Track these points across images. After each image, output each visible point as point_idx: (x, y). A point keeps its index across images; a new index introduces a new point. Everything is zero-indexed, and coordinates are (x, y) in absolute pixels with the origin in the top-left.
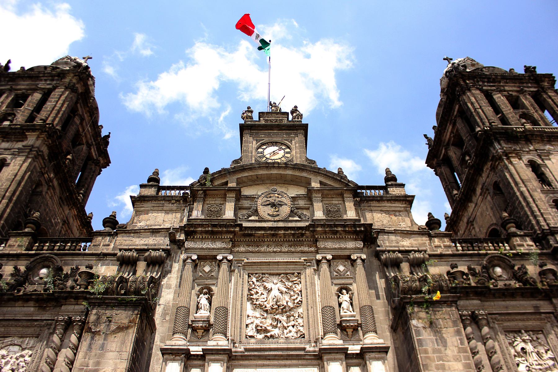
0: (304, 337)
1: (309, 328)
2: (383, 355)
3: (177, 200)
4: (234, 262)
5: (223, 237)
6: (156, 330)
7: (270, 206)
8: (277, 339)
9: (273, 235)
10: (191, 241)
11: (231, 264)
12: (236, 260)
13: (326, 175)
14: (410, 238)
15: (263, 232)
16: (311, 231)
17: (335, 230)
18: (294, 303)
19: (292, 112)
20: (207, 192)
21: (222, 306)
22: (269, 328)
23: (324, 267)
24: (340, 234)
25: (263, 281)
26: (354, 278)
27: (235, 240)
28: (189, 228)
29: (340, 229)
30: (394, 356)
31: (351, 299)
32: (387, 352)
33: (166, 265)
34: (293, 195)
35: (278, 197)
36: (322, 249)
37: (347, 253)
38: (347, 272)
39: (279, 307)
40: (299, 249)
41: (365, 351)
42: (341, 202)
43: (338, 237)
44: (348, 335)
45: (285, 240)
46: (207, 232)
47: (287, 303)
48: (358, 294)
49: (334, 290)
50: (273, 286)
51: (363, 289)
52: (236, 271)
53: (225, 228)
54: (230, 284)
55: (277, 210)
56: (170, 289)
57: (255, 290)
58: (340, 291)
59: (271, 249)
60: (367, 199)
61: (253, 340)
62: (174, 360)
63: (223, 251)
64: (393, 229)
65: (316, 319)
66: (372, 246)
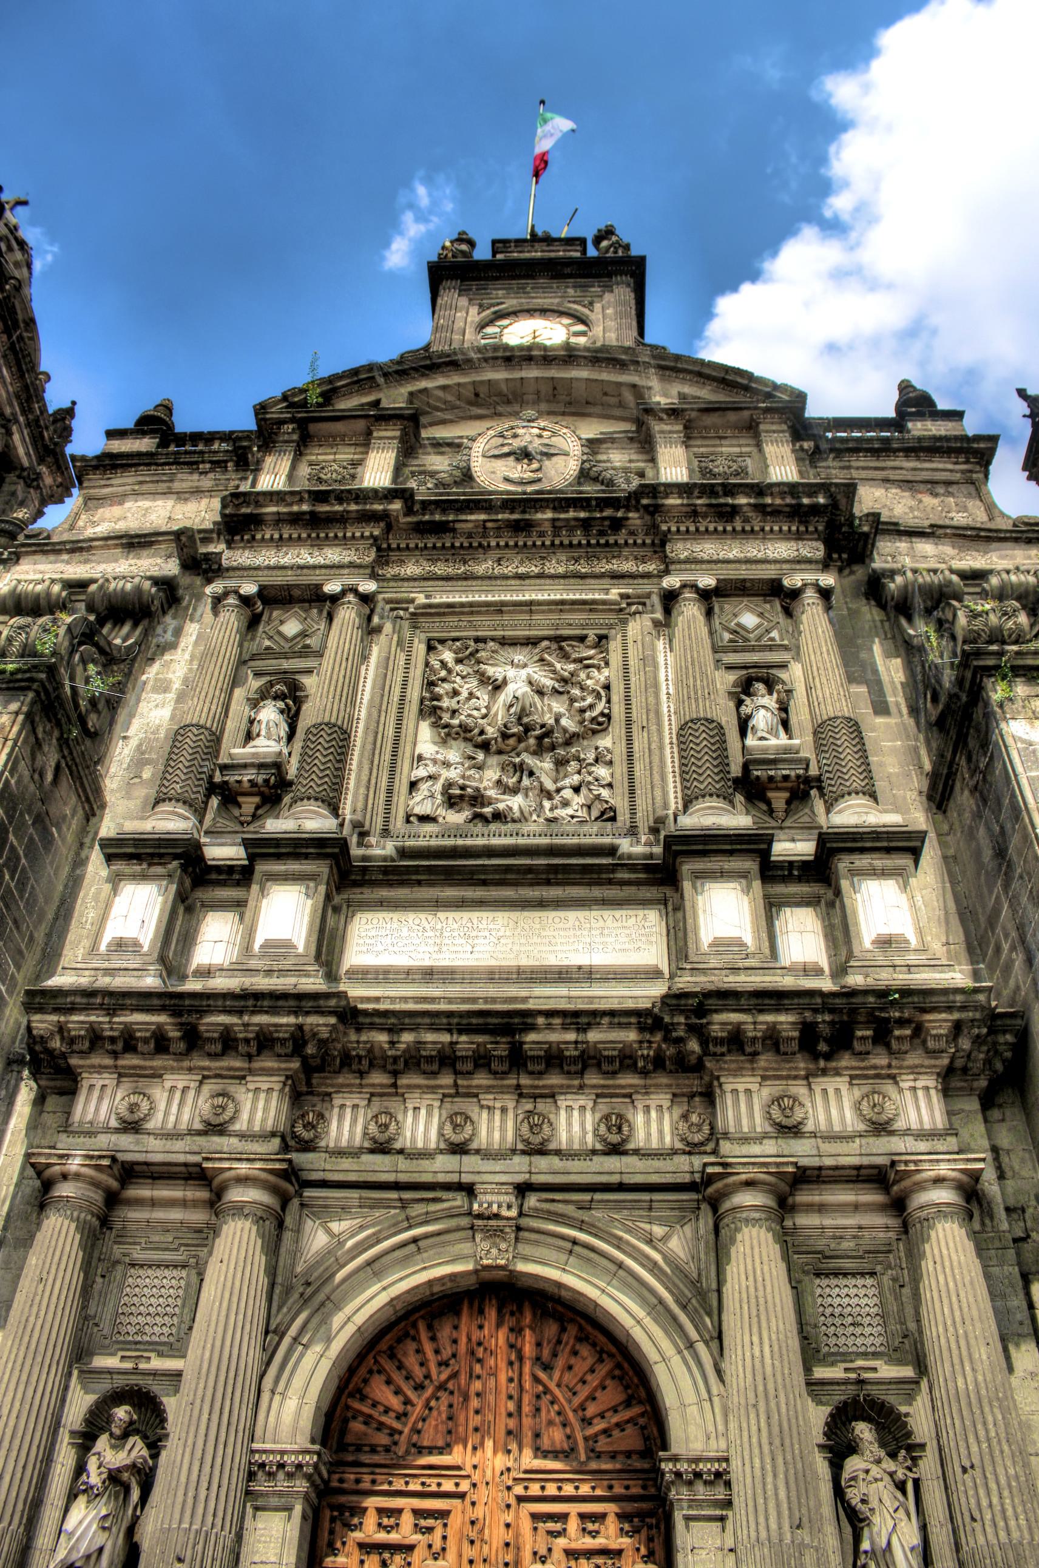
0: (613, 819)
1: (632, 792)
2: (906, 861)
3: (218, 462)
4: (380, 605)
5: (349, 534)
6: (103, 806)
7: (512, 458)
8: (518, 826)
9: (520, 527)
10: (244, 548)
11: (372, 611)
12: (388, 601)
13: (700, 374)
14: (986, 553)
15: (483, 517)
16: (646, 507)
17: (727, 505)
18: (581, 722)
19: (598, 240)
20: (313, 428)
21: (326, 720)
22: (492, 793)
23: (690, 611)
24: (746, 520)
25: (479, 662)
26: (796, 651)
27: (389, 545)
28: (237, 506)
29: (742, 500)
30: (943, 882)
31: (784, 708)
32: (915, 853)
33: (159, 630)
34: (591, 436)
35: (540, 436)
36: (680, 562)
37: (768, 572)
38: (768, 631)
39: (528, 729)
40: (604, 567)
41: (835, 845)
42: (748, 449)
43: (739, 528)
44: (771, 812)
45: (557, 542)
46: (295, 519)
47: (557, 721)
48: (809, 689)
49: (722, 683)
50: (511, 673)
51: (826, 669)
52: (388, 627)
53: (357, 503)
54: (364, 667)
55: (535, 466)
56: (165, 691)
57: (447, 686)
58: (745, 688)
59: (509, 569)
60: (838, 445)
61: (429, 828)
62: (143, 877)
63: (346, 571)
64: (927, 523)
65: (656, 759)
66: (855, 568)
